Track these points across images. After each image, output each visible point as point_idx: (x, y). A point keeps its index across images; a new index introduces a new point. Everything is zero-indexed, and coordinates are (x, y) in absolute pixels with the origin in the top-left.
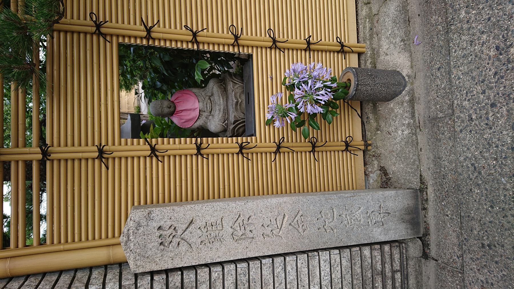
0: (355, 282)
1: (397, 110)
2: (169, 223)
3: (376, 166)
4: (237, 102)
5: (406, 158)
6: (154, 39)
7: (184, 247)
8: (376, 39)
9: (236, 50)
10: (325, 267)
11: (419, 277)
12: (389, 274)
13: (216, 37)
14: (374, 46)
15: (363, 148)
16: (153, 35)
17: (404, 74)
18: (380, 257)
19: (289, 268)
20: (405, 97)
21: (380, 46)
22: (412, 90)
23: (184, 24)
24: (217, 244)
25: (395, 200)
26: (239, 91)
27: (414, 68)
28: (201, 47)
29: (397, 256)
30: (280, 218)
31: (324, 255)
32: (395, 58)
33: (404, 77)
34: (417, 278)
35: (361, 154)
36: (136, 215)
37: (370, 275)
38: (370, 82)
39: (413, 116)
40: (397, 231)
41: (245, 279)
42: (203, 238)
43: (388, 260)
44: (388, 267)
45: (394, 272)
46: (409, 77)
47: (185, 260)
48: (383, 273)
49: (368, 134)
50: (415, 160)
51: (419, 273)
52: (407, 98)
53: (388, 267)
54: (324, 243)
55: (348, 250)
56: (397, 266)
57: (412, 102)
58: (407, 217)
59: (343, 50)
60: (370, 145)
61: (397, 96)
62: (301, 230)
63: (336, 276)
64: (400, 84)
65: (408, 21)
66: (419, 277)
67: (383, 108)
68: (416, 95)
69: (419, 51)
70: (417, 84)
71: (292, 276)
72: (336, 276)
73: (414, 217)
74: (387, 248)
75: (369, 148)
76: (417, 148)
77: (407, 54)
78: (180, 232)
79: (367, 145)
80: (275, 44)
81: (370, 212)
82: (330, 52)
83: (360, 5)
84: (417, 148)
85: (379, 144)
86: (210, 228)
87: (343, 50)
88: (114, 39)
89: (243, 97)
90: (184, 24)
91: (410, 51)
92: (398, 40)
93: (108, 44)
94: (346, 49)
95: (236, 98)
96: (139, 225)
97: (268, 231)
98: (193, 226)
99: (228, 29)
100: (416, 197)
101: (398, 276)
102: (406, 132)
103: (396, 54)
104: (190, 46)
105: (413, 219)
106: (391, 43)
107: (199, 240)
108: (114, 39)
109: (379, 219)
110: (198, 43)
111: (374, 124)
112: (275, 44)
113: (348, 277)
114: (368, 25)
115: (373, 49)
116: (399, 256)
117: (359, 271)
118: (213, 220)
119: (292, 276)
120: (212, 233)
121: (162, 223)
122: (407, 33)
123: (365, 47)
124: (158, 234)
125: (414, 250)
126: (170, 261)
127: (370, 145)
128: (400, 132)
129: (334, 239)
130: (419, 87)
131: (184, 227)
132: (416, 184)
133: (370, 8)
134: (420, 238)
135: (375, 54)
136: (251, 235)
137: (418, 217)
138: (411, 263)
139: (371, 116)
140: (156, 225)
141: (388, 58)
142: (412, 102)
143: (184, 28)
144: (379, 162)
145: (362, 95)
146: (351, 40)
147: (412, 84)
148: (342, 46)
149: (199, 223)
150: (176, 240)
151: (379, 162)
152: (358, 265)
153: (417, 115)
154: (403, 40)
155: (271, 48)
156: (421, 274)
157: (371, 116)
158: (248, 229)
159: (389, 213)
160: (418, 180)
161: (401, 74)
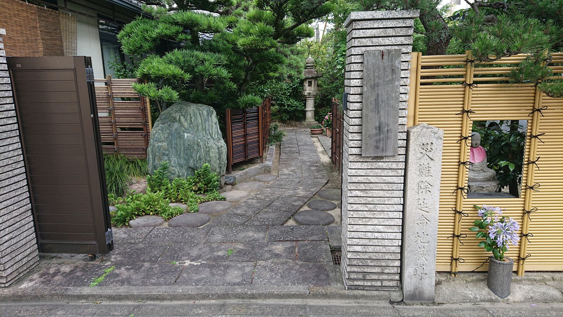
0: (380, 254)
1: (484, 292)
2: (434, 148)
3: (442, 279)
4: (483, 188)
5: (453, 295)
6: (530, 139)
7: (419, 155)
8: (528, 282)
9: (523, 188)
10: (392, 236)
11: (378, 298)
12: (381, 277)
13: (531, 175)
14: (523, 282)
15: (453, 271)
16: (533, 139)
17: (509, 297)
18: (393, 272)
19: (396, 213)
20: (494, 297)
21: (524, 284)
22: (499, 302)
23: (540, 156)
24: (418, 173)
25: (428, 285)
26: (490, 189)
27: (514, 304)
28: (525, 166)
29: (391, 284)
30: (427, 210)
31: (399, 236)
32: (519, 292)
33: (506, 297)
34: (377, 296)
35: (448, 269)
36: (441, 132)
37: (383, 264)
38: (505, 273)
39: (482, 301)
40: (409, 284)
41: (394, 188)
42: (422, 165)
43: (390, 277)
44: (385, 277)
45: (382, 281)
46: (507, 300)
47: (413, 156)
48: (382, 273)
49: (462, 275)
50: (453, 300)
51: (380, 298)
52: (493, 298)
53: (385, 277)
54: (409, 236)
55: (400, 251)
56: (386, 283)
57: (491, 301)
58: (417, 293)
59: (520, 259)
60: (455, 275)
61: (494, 292)
62: (418, 222)
63: (386, 243)
64: (502, 293)
65: (546, 301)
66: (378, 298)
67: (483, 285)
68: (496, 304)
69: (527, 306)
70: (504, 305)
71: (391, 215)
72: (386, 243)
73: (416, 297)
74: (397, 277)
75: (453, 275)
76: (461, 302)
77: (522, 300)
78: (428, 154)
79: (455, 274)
80: (526, 212)
81: (424, 267)
82: (519, 251)
83: (551, 274)
84: (461, 302)
85: (457, 282)
86: (427, 169)
87: (520, 259)
88: (531, 118)
89: (486, 192)
90: (540, 156)
91: (525, 302)
92: (532, 295)
93: (527, 115)
94: (521, 262)
95: (486, 187)
96: (435, 133)
97: (421, 202)
98: (429, 160)
99: (537, 183)
100: (429, 299)
101: (379, 284)
102: (471, 296)
103: (522, 293)
104: (526, 160)
105: (416, 296)
106: (529, 291)
107: (422, 164)
108: (531, 118)
109: (418, 273)
110: (528, 164)
111: (469, 280)
112: (526, 212)
113: (383, 250)
114: (538, 278)
115: (521, 281)
116: (391, 285)
117: (387, 258)
118: (432, 171)
119: (391, 215)
120: (424, 171)
121: (434, 144)
122: (537, 301)
123: (522, 275)
124: (429, 143)
125: (396, 296)
126: (413, 149)
127: (455, 275)
128: (470, 292)
129: (410, 242)
130: (501, 305)
131: (430, 156)
132: (438, 300)
133: (550, 281)
134: (402, 300)
135: (519, 282)
136: (420, 192)
137: (416, 300)
138: (387, 293)
139: (475, 278)
140: (434, 141)
141: (517, 288)
142: (491, 301)
143: (538, 156)
144: (444, 281)
145: (492, 269)
146: (527, 266)
147: (503, 302)
148: (524, 259)
149: (432, 163)
150: (424, 151)
151: (444, 281)
152: (390, 257)
153: (482, 303)
154: (532, 298)
155: (524, 210)
156: (380, 300)
157: (475, 278)
158: (424, 191)
159: (421, 280)
160: (440, 302)
161: (508, 295)
